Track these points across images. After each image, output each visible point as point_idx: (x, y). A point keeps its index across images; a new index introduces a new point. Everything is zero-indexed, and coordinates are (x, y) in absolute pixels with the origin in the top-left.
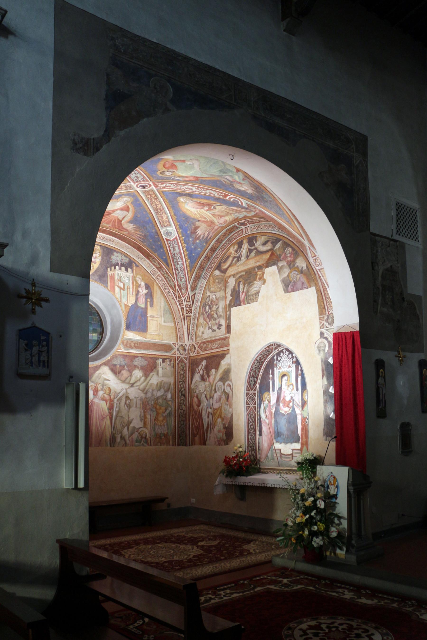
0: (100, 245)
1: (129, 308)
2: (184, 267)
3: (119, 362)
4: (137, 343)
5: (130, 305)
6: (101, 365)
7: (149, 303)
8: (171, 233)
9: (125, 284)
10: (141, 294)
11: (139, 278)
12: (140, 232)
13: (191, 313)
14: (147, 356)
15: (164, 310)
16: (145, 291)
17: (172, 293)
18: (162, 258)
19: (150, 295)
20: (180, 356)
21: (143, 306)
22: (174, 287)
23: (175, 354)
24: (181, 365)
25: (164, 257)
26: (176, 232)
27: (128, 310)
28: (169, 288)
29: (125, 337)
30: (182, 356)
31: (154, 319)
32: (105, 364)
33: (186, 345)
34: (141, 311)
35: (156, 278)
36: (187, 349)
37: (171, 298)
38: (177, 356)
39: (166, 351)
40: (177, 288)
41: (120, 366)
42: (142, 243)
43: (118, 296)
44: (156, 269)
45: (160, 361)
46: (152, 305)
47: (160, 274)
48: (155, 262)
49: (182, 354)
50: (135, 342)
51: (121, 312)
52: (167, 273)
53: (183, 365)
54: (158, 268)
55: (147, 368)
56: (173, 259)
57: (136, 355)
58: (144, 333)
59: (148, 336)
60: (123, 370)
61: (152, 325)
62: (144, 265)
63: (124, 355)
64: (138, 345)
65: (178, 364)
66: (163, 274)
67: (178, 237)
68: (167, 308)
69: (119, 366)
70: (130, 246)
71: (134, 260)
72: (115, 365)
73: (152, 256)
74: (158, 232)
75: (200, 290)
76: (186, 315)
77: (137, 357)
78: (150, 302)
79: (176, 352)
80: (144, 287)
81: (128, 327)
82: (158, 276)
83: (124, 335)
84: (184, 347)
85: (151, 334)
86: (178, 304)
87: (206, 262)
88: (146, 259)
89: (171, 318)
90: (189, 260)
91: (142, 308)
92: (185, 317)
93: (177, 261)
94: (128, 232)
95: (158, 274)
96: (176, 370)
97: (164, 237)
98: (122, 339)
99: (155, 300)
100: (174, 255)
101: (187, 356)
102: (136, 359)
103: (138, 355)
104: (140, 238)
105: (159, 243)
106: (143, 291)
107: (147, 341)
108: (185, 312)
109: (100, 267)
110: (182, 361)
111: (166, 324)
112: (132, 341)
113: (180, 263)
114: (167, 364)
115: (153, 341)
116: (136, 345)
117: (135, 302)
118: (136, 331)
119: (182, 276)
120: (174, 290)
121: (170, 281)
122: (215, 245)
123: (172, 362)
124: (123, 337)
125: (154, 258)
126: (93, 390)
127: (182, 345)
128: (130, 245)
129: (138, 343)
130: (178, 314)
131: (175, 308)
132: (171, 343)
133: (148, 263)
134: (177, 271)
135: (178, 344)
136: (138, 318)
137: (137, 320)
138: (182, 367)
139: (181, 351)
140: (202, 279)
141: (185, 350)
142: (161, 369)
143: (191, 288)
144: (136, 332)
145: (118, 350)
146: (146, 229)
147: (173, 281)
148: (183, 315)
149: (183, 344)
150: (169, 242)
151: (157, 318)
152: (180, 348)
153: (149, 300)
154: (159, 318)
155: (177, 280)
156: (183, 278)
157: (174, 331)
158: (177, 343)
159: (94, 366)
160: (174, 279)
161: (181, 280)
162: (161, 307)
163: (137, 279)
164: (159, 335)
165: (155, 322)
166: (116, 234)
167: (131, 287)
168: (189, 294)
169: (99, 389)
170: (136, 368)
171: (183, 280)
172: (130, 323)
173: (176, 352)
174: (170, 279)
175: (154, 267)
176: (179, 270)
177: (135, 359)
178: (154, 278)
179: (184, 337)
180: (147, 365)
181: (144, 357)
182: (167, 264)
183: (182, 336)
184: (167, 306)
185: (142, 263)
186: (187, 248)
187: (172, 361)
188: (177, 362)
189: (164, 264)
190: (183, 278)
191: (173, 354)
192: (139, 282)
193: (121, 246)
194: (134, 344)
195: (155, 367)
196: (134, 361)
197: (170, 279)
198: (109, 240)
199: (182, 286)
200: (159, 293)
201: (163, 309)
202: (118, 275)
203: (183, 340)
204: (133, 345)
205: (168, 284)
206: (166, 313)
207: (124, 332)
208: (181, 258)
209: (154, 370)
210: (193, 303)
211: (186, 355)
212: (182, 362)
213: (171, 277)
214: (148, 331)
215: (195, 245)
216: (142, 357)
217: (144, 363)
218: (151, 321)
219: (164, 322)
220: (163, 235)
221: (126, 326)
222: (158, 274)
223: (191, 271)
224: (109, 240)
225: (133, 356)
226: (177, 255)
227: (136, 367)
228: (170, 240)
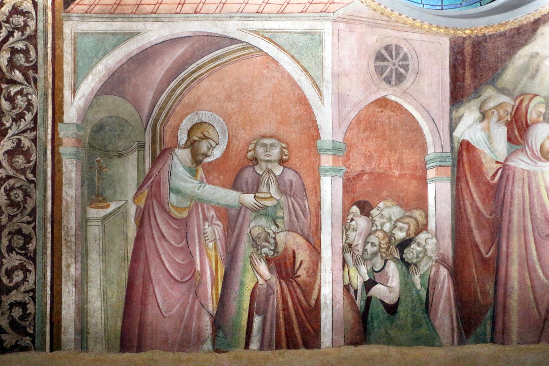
126: (509, 124)
159: (508, 27)
169: (532, 115)
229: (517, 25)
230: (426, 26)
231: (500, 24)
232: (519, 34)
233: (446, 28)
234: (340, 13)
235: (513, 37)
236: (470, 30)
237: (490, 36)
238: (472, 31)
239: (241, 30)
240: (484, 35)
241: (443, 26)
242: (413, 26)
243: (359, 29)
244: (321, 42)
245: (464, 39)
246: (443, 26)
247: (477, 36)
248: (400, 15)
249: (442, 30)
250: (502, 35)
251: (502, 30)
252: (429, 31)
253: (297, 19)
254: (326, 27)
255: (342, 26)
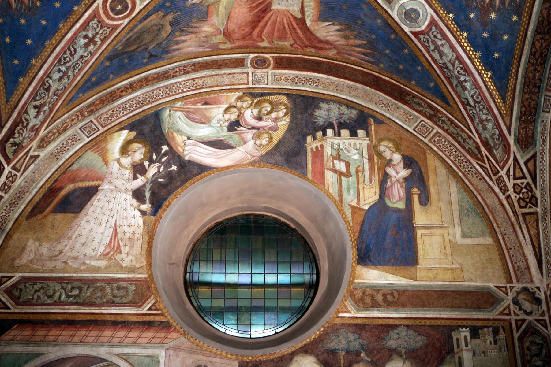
0: (287, 95)
1: (363, 213)
2: (481, 93)
3: (344, 342)
4: (392, 294)
5: (366, 207)
6: (293, 355)
7: (416, 199)
8: (414, 11)
9: (351, 162)
10: (394, 179)
11: (387, 149)
12: (355, 38)
13: (536, 205)
14: (423, 323)
15: (461, 209)
16: (404, 173)
17: (478, 167)
18: (429, 89)
19: (418, 180)
20: (526, 317)
21: (401, 205)
22: (476, 151)
23: (509, 314)
24: (533, 343)
25: (432, 85)
26: (427, 6)
27: (360, 220)
28: (469, 158)
29: (356, 281)
30: (529, 318)
31: (433, 231)
32: (305, 350)
33: (538, 288)
34: (394, 216)
35: (430, 141)
36: (543, 297)
37: (475, 181)
38: (513, 318)
39: (478, 308)
40: (483, 149)
41: (348, 352)
42: (374, 67)
43: (333, 190)
44: (427, 121)
45: (463, 335)
46: (425, 201)
47: (440, 131)
48: (420, 105)
49: (530, 314)
50: (385, 291)
51: (343, 226)
52: (452, 122)
53: (538, 340)
54: (430, 118)
55: (425, 353)
56: (448, 79)
57: (391, 322)
58: (408, 268)
59: (420, 274)
60: (358, 362)
61: (431, 250)
62: (397, 118)
63: (356, 325)
64: (393, 298)
65: (521, 339)
66: (446, 128)
67: (437, 18)
68: (468, 202)
69: (344, 353)
70: (358, 85)
71: (370, 112)
72: (333, 352)
73: (408, 94)
74: (390, 21)
75: (543, 142)
76: (520, 211)
77: (395, 327)
78: (420, 196)
79: (509, 305)
80: (402, 165)
81: (364, 258)
82: (434, 136)
83: (354, 276)
84: (534, 293)
85: (430, 269)
86: (497, 190)
87: (539, 68)
88: (400, 104)
89: (481, 226)
90: (489, 73)
91: (398, 210)
92: (521, 218)
93: (460, 82)
94: (335, 47)
95: (435, 131)
96: (518, 356)
97: (407, 30)
98: (349, 286)
99: (433, 190)
100: (447, 68)
101: (546, 318)
102: (393, 334)
103: (397, 322)
104: (364, 54)
105: (406, 51)
106: (399, 173)
107: (420, 286)
108: (516, 204)
109: (288, 136)
110: (531, 331)
111: (469, 241)
112: (376, 289)
113: (468, 85)
114: (485, 341)
115: (437, 284)
116: (390, 298)
117: (377, 197)
118: (387, 264)
119: (484, 117)
120: (478, 159)
121: (464, 140)
122: (545, 13)
123: (502, 336)
124: (351, 282)
125: (414, 96)
127: (525, 289)
128: (357, 82)
129: (396, 294)
130: (502, 215)
131: (491, 200)
132: (492, 285)
133: (405, 112)
134: (468, 108)
135: (512, 288)
136: (389, 233)
137: (388, 237)
138: (534, 348)
139: (527, 306)
140: (542, 114)
141: (538, 301)
142: (470, 354)
143: (518, 141)
144: (386, 267)
145: (341, 315)
146: (363, 24)
147: (470, 137)
148: (515, 213)
149: (529, 286)
150: (421, 37)
151: (442, 228)
152: (521, 297)
153: (415, 190)
154: (447, 228)
155: (477, 131)
156: (488, 121)
157: (496, 256)
158: (508, 285)
159: (275, 356)
160: (471, 131)
161: (485, 128)
162: (450, 203)
163: (382, 148)
164: (452, 269)
165: (436, 240)
166: (318, 63)
167: (367, 167)
168: (515, 159)
170: (394, 356)
171: (490, 126)
172: (368, 247)
173: (509, 305)
174: (463, 134)
175: (422, 118)
176: (472, 103)
177: (388, 332)
178: (426, 141)
179: (528, 268)
180: (427, 346)
181: (414, 326)
182: (445, 99)
183: (523, 265)
184: (467, 198)
185: (392, 115)
186: (472, 41)
187: (502, 331)
188: (516, 335)
189: (438, 101)
190: (488, 121)
191: (501, 313)
192: (387, 154)
193: (338, 88)
194: (385, 296)
195: (451, 351)
196: (387, 338)
197: (463, 134)
198: (306, 81)
199: (490, 140)
200: (442, 171)
201: (456, 207)
202: (333, 147)
203: (527, 276)
204: (380, 298)
205: (464, 148)
206: (467, 215)
207: (354, 271)
208: (467, 71)
209: (448, 358)
210: (534, 179)
211: (543, 314)
212: (532, 334)
213: (462, 129)
214: (420, 261)
215: (489, 27)
216: (408, 326)
217: (418, 341)
218: (426, 238)
219: (464, 236)
220: (403, 26)
221: (359, 255)
222: (435, 131)
223: (503, 99)
224: (306, 81)
225: (381, 325)
226: (453, 65)
227: (392, 353)
228: (422, 33)
229: (280, 355)
230: (224, 354)
231: (271, 354)
232: (282, 360)
233: (237, 355)
234: (171, 344)
235: (278, 362)
236: (252, 357)
237: (264, 361)
238: (253, 358)
239: (108, 353)
240: (260, 360)
241: (235, 354)
242: (216, 354)
243: (182, 354)
244: (158, 362)
245: (248, 362)
246: (235, 354)
247: (256, 361)
248: (208, 346)
249: (234, 357)
250: (271, 361)
251: (271, 357)
252: (226, 357)
253: (144, 347)
254: (162, 353)
255: (172, 352)
